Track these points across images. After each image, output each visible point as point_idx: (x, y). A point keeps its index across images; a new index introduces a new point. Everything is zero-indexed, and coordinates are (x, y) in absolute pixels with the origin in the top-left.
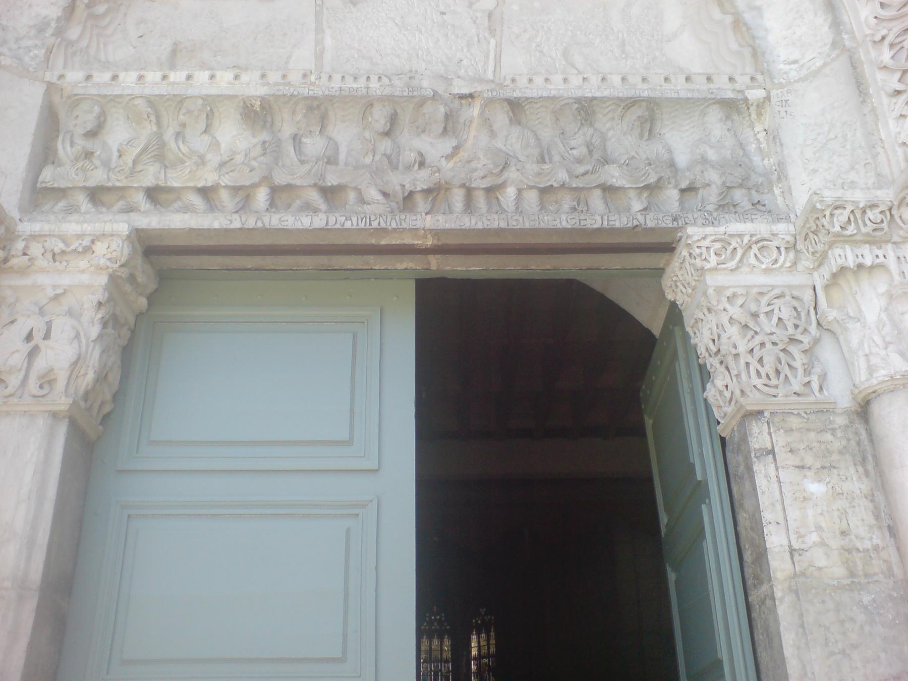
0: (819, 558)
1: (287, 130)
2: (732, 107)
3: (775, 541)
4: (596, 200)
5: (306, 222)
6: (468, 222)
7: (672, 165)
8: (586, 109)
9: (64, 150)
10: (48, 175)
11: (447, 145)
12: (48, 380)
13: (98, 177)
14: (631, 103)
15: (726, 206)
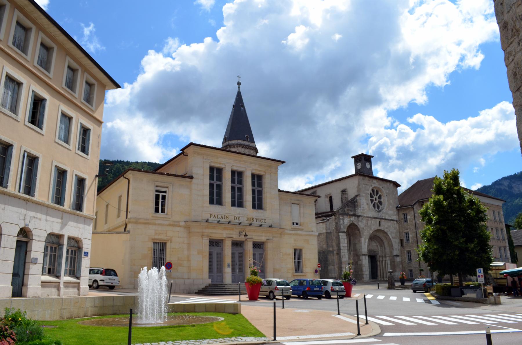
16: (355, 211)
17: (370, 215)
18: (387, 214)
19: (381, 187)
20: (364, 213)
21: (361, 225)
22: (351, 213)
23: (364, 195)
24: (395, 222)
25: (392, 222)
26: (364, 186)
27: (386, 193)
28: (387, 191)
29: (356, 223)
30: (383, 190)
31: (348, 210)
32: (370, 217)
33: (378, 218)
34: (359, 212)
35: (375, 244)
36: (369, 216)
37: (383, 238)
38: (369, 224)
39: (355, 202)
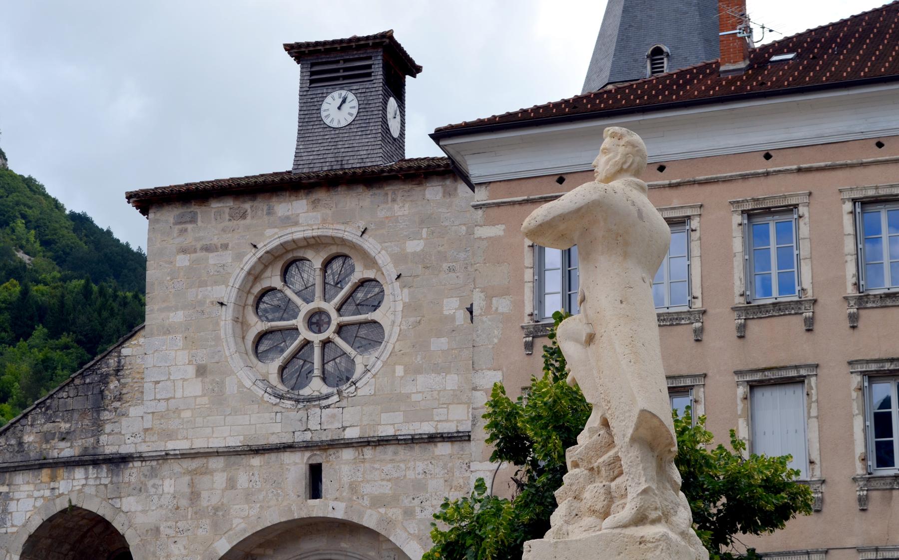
16: (98, 428)
18: (393, 401)
19: (350, 233)
20: (170, 435)
22: (66, 451)
23: (178, 317)
25: (443, 449)
26: (183, 261)
27: (399, 258)
28: (414, 246)
30: (370, 244)
31: (47, 437)
32: (217, 453)
34: (125, 433)
36: (217, 443)
38: (208, 499)
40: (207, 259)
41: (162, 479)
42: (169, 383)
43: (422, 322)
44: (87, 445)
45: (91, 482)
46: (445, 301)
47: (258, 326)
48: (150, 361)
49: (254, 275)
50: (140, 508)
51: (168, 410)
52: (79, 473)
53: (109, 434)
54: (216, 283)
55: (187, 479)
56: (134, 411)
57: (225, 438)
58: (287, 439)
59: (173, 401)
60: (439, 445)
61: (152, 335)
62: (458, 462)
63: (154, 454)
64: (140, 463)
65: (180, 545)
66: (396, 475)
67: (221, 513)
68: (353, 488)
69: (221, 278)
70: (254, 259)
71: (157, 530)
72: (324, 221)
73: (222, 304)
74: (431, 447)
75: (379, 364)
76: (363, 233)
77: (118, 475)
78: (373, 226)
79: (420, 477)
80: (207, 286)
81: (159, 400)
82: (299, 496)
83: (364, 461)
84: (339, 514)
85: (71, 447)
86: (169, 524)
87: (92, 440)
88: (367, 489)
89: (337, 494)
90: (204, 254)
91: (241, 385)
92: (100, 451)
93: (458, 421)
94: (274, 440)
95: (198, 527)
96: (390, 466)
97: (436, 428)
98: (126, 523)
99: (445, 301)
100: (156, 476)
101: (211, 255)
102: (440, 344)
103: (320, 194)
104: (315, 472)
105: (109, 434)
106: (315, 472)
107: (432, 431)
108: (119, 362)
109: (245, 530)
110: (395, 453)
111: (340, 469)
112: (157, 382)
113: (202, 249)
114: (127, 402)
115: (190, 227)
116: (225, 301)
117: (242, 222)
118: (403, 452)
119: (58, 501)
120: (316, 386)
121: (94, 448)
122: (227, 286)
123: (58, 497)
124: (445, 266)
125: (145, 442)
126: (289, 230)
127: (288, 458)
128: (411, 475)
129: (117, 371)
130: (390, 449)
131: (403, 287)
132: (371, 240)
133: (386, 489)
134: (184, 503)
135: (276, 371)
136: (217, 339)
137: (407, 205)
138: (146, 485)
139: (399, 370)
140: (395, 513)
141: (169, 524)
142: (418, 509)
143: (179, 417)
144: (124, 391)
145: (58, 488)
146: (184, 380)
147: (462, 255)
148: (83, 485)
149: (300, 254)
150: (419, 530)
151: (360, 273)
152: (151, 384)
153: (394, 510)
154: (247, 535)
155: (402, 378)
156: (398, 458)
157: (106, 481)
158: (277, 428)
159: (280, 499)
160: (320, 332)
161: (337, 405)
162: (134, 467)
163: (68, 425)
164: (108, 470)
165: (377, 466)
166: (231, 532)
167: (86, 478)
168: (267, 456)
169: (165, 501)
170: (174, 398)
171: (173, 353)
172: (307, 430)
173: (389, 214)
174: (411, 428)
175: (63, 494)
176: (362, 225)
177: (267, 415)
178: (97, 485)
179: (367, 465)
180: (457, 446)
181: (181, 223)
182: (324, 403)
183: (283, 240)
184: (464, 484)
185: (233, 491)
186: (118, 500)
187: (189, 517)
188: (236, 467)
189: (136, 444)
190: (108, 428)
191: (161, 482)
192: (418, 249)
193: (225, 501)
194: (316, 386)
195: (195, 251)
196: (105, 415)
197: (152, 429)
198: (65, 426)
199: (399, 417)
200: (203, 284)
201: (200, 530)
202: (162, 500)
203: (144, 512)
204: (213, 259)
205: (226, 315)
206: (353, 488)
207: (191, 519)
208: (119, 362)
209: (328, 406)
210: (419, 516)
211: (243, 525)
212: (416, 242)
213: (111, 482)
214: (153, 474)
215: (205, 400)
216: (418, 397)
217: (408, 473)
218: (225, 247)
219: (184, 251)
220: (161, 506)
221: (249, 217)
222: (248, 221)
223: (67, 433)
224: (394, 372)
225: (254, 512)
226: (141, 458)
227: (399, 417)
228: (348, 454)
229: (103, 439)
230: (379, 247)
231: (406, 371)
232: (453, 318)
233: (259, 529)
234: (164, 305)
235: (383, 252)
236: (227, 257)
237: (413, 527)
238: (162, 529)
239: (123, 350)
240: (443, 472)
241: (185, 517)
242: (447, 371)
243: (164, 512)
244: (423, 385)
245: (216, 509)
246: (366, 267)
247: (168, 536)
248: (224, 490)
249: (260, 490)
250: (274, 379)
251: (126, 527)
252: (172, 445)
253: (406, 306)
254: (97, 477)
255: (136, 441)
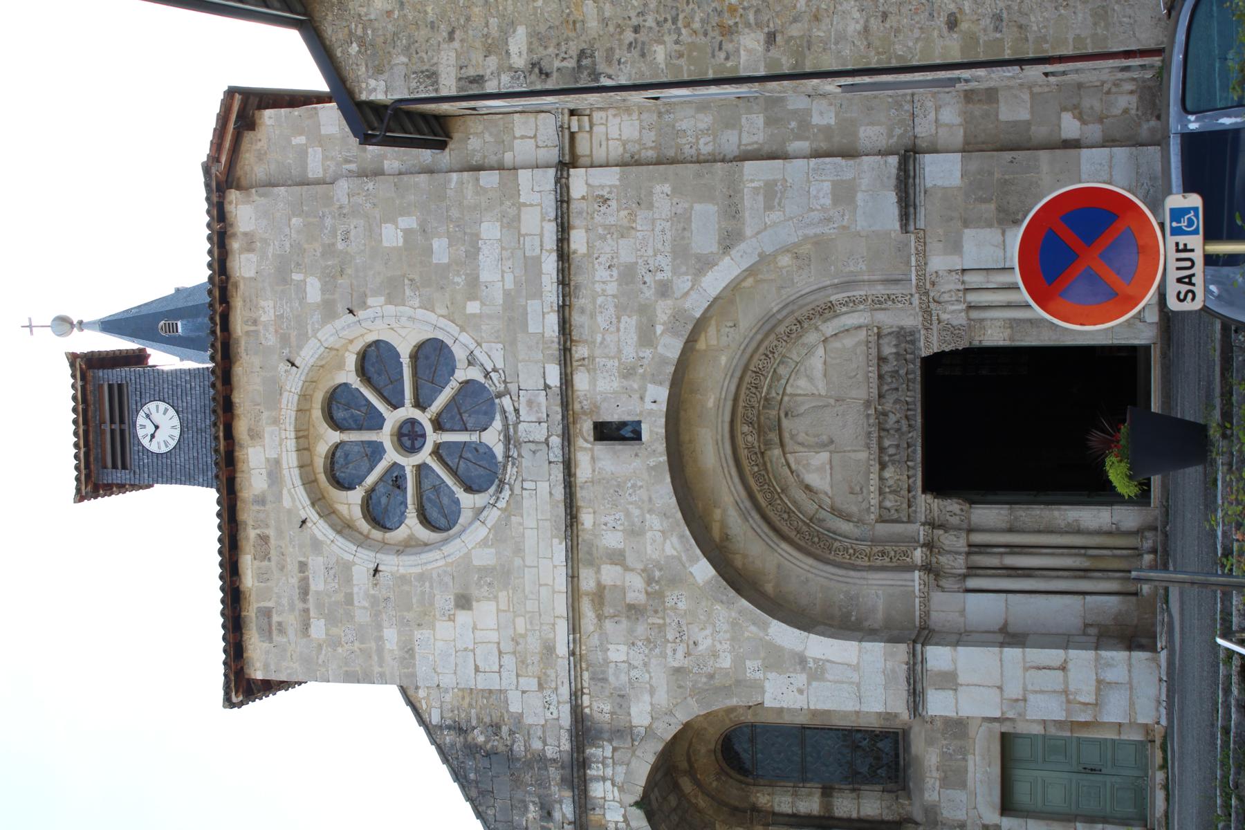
0: (1006, 334)
1: (887, 458)
2: (879, 336)
3: (1001, 343)
4: (911, 376)
5: (919, 450)
6: (919, 410)
7: (897, 354)
8: (880, 377)
9: (896, 516)
10: (905, 519)
11: (891, 415)
12: (962, 510)
13: (905, 506)
14: (879, 366)
15: (913, 342)
17: (547, 562)
18: (513, 318)
19: (293, 383)
20: (549, 649)
21: (652, 701)
23: (391, 635)
24: (579, 181)
25: (578, 241)
26: (318, 629)
27: (328, 310)
28: (314, 291)
29: (642, 768)
30: (308, 356)
32: (573, 578)
33: (568, 466)
35: (817, 362)
36: (561, 582)
37: (747, 318)
39: (472, 749)
40: (317, 593)
41: (607, 662)
42: (478, 651)
43: (411, 276)
44: (558, 777)
45: (609, 772)
46: (385, 244)
47: (411, 525)
48: (448, 680)
49: (344, 528)
50: (647, 698)
51: (514, 653)
52: (597, 790)
53: (545, 744)
54: (349, 580)
55: (609, 625)
56: (515, 707)
57: (555, 567)
58: (558, 473)
59: (502, 645)
60: (573, 246)
61: (414, 675)
62: (598, 219)
63: (572, 673)
64: (585, 697)
65: (699, 637)
66: (612, 310)
67: (657, 574)
68: (628, 372)
69: (344, 571)
70: (322, 524)
71: (678, 671)
72: (276, 421)
73: (376, 571)
74: (575, 259)
75: (464, 338)
76: (293, 365)
77: (601, 731)
78: (286, 351)
79: (615, 273)
80: (351, 594)
81: (501, 666)
82: (636, 455)
83: (592, 358)
84: (661, 393)
85: (561, 802)
86: (669, 652)
87: (552, 770)
88: (629, 352)
89: (636, 396)
90: (311, 598)
91: (484, 543)
92: (566, 758)
93: (543, 219)
94: (559, 492)
95: (674, 609)
96: (599, 319)
97: (550, 251)
98: (667, 719)
99: (385, 244)
100: (603, 672)
101: (313, 587)
102: (441, 250)
103: (242, 428)
104: (607, 432)
105: (545, 744)
106: (607, 432)
107: (554, 256)
108: (449, 728)
109: (682, 537)
110: (583, 311)
111: (602, 391)
112: (477, 669)
113: (305, 601)
114: (502, 715)
115: (276, 618)
116: (373, 566)
117: (272, 542)
118: (580, 302)
119: (633, 824)
120: (492, 438)
121: (563, 767)
122: (354, 564)
123: (628, 825)
124: (340, 246)
125: (556, 689)
126: (286, 472)
127: (583, 471)
128: (612, 288)
129: (460, 730)
130: (577, 318)
131: (364, 305)
132: (303, 353)
133: (630, 323)
134: (641, 629)
135: (471, 496)
136: (421, 577)
137: (262, 303)
138: (615, 689)
139: (473, 307)
140: (663, 311)
141: (669, 652)
142: (659, 276)
143: (524, 636)
144: (487, 720)
145: (617, 823)
146: (475, 628)
147: (328, 222)
148: (613, 785)
149: (319, 463)
150: (686, 274)
151: (348, 375)
152: (479, 678)
153: (659, 312)
154: (688, 533)
155: (483, 304)
156: (589, 307)
157: (608, 753)
158: (543, 487)
159: (640, 484)
160: (424, 436)
161: (515, 398)
162: (590, 706)
163: (531, 807)
164: (594, 745)
165: (599, 338)
166: (684, 558)
167: (604, 779)
168: (580, 503)
169: (638, 660)
170: (499, 643)
171: (439, 644)
172: (547, 442)
173: (272, 329)
174: (549, 288)
175: (624, 816)
176: (283, 367)
177: (526, 503)
178: (614, 763)
179: (597, 352)
180: (575, 221)
181: (270, 632)
182: (512, 417)
183: (298, 482)
184: (626, 208)
185: (627, 554)
186: (635, 730)
187: (661, 621)
188: (594, 549)
189: (559, 702)
190: (537, 745)
191: (612, 665)
192: (318, 285)
193: (640, 566)
194: (492, 438)
195: (307, 611)
196: (519, 748)
197: (539, 678)
198: (533, 812)
199: (533, 306)
200: (349, 600)
201: (680, 604)
202: (635, 663)
203: (652, 692)
204: (317, 585)
205: (391, 564)
206: (628, 372)
207: (664, 619)
208: (449, 728)
209: (517, 411)
210: (667, 275)
211: (675, 539)
212: (309, 289)
213: (610, 741)
214: (600, 679)
215: (503, 595)
216: (509, 278)
217: (610, 292)
218: (303, 566)
219: (306, 626)
220: (645, 665)
221: (267, 532)
222: (271, 532)
223: (541, 808)
224: (474, 315)
225: (654, 521)
226: (576, 695)
227: (533, 306)
228: (581, 381)
229: (550, 752)
230: (313, 343)
231: (472, 297)
232: (408, 233)
233: (679, 515)
234: (375, 658)
235: (319, 335)
236: (316, 563)
237: (683, 283)
238: (676, 664)
239: (434, 722)
240: (610, 241)
241: (661, 628)
242: (476, 237)
243: (653, 661)
244: (494, 273)
245: (650, 581)
246: (341, 366)
247: (687, 654)
248: (627, 569)
249: (628, 514)
250: (480, 499)
251: (673, 720)
252: (562, 650)
253: (390, 300)
254: (603, 763)
255: (555, 703)
